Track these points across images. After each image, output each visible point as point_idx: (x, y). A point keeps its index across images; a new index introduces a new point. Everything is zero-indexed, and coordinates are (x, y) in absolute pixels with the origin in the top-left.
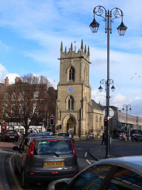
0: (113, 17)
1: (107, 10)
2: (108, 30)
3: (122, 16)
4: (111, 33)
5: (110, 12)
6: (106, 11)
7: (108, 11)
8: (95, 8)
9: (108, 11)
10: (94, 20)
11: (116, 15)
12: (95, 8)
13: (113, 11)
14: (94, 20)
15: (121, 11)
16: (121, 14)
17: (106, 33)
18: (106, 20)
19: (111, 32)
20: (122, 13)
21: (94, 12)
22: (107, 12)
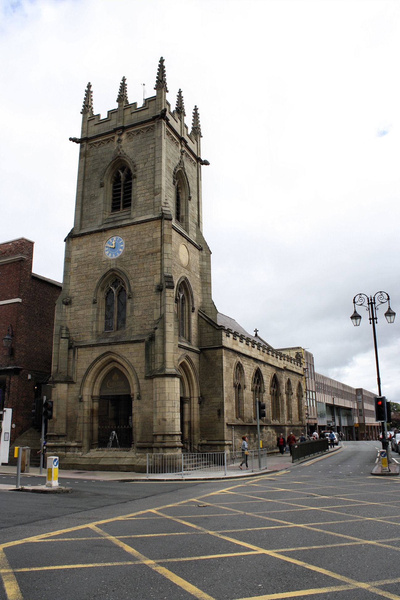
0: (377, 302)
1: (369, 297)
2: (373, 319)
3: (388, 299)
4: (377, 323)
5: (373, 299)
6: (368, 299)
7: (371, 298)
8: (355, 298)
9: (371, 298)
10: (355, 312)
11: (381, 301)
12: (355, 298)
13: (376, 297)
14: (355, 312)
15: (387, 294)
16: (387, 298)
17: (371, 323)
18: (369, 309)
19: (376, 322)
20: (388, 296)
21: (354, 302)
22: (370, 299)
